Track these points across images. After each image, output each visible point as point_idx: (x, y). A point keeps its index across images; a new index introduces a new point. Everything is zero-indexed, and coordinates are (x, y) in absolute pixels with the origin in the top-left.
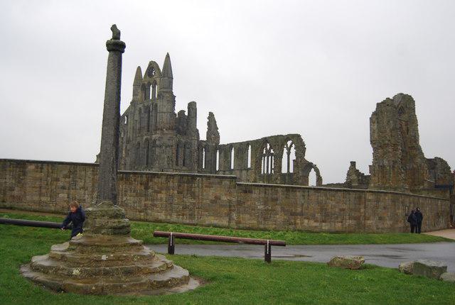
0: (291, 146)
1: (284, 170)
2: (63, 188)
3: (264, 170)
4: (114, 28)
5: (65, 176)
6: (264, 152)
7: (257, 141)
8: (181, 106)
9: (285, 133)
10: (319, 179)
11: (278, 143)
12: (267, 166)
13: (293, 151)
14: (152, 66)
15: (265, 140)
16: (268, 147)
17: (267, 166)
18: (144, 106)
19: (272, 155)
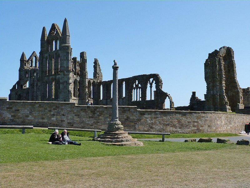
0: (153, 82)
1: (148, 98)
2: (54, 115)
3: (134, 99)
4: (114, 61)
5: (54, 109)
6: (134, 86)
9: (148, 73)
10: (172, 103)
11: (144, 80)
12: (136, 96)
13: (154, 85)
14: (53, 27)
15: (135, 78)
17: (136, 96)
19: (139, 88)
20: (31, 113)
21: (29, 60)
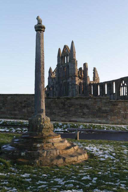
2: (25, 107)
3: (122, 94)
4: (38, 18)
6: (122, 85)
7: (118, 80)
8: (80, 65)
14: (65, 47)
15: (122, 79)
16: (123, 82)
18: (63, 66)
19: (125, 86)
20: (3, 105)
21: (54, 71)
